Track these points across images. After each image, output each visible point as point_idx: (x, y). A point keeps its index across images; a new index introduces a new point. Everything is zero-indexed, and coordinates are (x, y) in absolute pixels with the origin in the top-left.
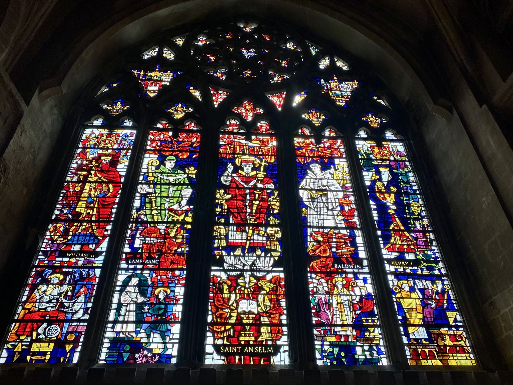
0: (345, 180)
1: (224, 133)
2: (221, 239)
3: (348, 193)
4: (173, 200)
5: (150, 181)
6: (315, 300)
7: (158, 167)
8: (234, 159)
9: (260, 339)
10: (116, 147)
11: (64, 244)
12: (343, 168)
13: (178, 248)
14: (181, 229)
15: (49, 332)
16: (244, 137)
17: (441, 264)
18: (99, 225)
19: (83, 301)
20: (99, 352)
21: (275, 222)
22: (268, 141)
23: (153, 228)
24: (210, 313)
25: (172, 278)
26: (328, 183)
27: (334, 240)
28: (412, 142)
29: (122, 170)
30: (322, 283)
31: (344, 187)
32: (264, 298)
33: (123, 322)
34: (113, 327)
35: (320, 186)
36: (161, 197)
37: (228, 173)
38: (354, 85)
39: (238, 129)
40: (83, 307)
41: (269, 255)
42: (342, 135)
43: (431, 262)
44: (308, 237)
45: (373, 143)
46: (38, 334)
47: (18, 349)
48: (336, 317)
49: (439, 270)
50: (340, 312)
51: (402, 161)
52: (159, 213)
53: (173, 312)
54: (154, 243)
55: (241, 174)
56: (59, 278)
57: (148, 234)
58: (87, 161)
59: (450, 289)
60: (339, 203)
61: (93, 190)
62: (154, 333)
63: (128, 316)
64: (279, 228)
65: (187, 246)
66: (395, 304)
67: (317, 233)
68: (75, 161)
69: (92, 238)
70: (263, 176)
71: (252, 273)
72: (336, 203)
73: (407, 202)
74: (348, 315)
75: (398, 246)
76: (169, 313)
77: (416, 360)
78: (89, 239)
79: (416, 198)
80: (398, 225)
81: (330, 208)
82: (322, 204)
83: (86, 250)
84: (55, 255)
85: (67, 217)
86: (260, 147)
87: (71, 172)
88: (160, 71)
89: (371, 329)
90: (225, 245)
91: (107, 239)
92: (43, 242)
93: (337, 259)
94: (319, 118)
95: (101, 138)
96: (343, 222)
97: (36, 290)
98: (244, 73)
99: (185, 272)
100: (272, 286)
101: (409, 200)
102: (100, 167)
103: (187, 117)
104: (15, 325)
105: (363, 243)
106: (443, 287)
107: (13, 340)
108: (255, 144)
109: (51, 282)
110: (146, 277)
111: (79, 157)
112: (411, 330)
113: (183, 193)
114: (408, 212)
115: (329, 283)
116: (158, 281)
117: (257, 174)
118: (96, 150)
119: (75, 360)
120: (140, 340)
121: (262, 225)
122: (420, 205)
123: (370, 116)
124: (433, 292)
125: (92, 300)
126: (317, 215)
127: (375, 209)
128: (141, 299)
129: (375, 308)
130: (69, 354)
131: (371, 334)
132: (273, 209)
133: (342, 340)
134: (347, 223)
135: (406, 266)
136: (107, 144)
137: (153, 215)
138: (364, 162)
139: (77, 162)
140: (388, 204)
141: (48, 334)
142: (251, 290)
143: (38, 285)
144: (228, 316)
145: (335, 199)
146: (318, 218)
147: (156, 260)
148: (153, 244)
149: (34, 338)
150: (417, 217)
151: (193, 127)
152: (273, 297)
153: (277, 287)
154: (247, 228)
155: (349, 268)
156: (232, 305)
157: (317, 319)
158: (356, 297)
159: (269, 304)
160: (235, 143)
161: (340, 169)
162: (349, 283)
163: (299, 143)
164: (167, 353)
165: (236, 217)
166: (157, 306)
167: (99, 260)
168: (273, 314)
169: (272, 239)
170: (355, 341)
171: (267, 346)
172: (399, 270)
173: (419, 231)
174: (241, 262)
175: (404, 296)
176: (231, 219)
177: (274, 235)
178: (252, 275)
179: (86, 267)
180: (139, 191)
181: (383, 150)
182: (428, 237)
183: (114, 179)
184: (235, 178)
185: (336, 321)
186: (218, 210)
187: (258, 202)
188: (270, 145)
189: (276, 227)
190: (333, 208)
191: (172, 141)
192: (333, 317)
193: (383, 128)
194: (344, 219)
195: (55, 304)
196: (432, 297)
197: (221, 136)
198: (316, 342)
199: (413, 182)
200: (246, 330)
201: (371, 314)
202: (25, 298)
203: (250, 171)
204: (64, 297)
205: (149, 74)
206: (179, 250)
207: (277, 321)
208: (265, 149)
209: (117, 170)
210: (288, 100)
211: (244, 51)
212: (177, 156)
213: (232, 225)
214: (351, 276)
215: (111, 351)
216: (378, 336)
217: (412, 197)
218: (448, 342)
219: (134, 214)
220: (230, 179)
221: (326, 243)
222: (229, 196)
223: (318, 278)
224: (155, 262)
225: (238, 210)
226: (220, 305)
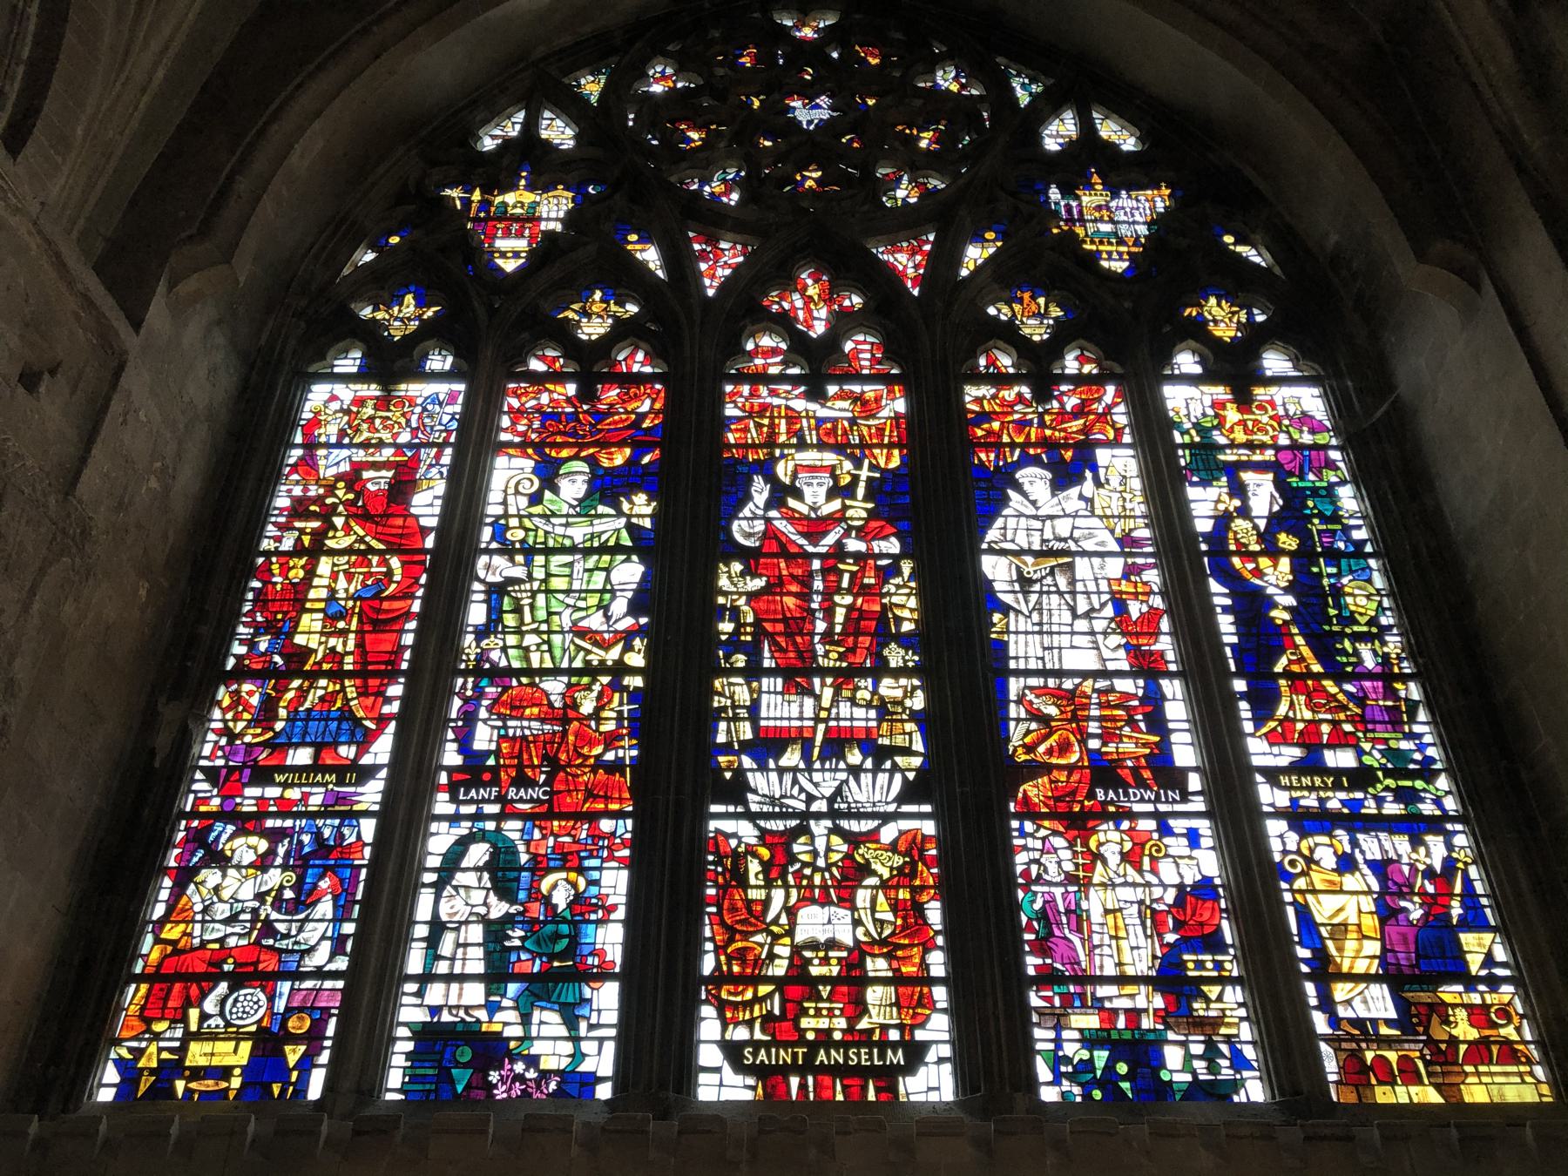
0: (1130, 517)
1: (740, 378)
2: (736, 718)
3: (1140, 561)
4: (585, 599)
5: (513, 543)
6: (1033, 902)
7: (536, 499)
8: (772, 461)
9: (863, 1024)
10: (405, 437)
11: (264, 744)
12: (1124, 477)
13: (605, 751)
14: (614, 691)
15: (234, 1010)
16: (802, 389)
17: (1443, 783)
18: (365, 686)
19: (330, 916)
20: (383, 1067)
21: (905, 661)
22: (878, 399)
23: (529, 690)
24: (709, 946)
25: (589, 841)
26: (1074, 528)
27: (1095, 712)
28: (1349, 383)
29: (429, 511)
30: (1056, 850)
31: (1127, 541)
32: (874, 900)
33: (449, 978)
34: (420, 994)
35: (1048, 541)
36: (548, 592)
37: (753, 508)
38: (1158, 199)
39: (782, 363)
40: (329, 933)
41: (888, 765)
42: (1118, 370)
43: (1412, 775)
44: (1012, 706)
45: (1220, 392)
46: (204, 1017)
47: (149, 1061)
48: (1101, 955)
49: (1438, 802)
50: (1111, 937)
51: (1316, 447)
52: (544, 642)
53: (597, 947)
54: (532, 735)
55: (794, 510)
56: (255, 848)
57: (513, 708)
58: (320, 486)
59: (1474, 862)
60: (1112, 592)
61: (341, 576)
62: (543, 1009)
63: (464, 959)
64: (920, 679)
65: (634, 742)
66: (1290, 911)
67: (1041, 691)
68: (283, 488)
69: (345, 726)
70: (864, 514)
71: (834, 823)
72: (1099, 593)
73: (1332, 581)
74: (1138, 948)
75: (1300, 726)
76: (586, 950)
77: (1356, 1086)
78: (339, 728)
79: (1363, 569)
80: (1302, 659)
81: (1080, 611)
82: (1055, 598)
83: (329, 762)
84: (239, 780)
85: (271, 662)
86: (853, 421)
87: (274, 524)
88: (531, 187)
89: (1213, 991)
90: (749, 735)
91: (392, 726)
92: (204, 741)
93: (1104, 771)
94: (1045, 315)
95: (358, 412)
96: (1122, 653)
97: (192, 886)
98: (799, 178)
99: (629, 822)
100: (898, 861)
101: (1339, 575)
102: (360, 504)
103: (622, 331)
104: (137, 990)
105: (1188, 721)
106: (1449, 857)
107: (134, 1033)
108: (839, 409)
109: (234, 862)
110: (513, 841)
111: (295, 477)
112: (1340, 991)
113: (616, 577)
114: (1335, 616)
115: (1079, 849)
116: (549, 851)
117: (845, 508)
118: (345, 453)
119: (315, 1091)
120: (502, 1032)
121: (863, 672)
122: (1378, 590)
123: (1213, 301)
124: (1417, 870)
125: (355, 914)
126: (1041, 633)
127: (1226, 610)
128: (499, 909)
129: (1225, 924)
130: (295, 1075)
131: (1212, 1005)
132: (899, 620)
133: (1121, 1023)
134: (1136, 657)
135: (1326, 788)
136: (377, 431)
137: (527, 650)
138: (1191, 455)
139: (289, 491)
140: (1270, 590)
141: (234, 1016)
142: (832, 876)
143: (196, 870)
144: (763, 956)
145: (1096, 579)
146: (1042, 643)
147: (541, 787)
148: (531, 739)
149: (193, 1027)
150: (1365, 629)
151: (639, 363)
152: (904, 894)
153: (913, 864)
154: (817, 681)
155: (1142, 800)
156: (775, 921)
157: (1039, 961)
158: (1165, 890)
159: (889, 917)
160: (772, 412)
161: (1115, 482)
162: (1143, 845)
163: (978, 400)
164: (582, 1068)
165: (781, 650)
166: (550, 928)
167: (371, 794)
168: (903, 947)
169: (897, 713)
170: (1161, 1027)
171: (884, 1045)
172: (1303, 802)
173: (1370, 676)
174: (802, 790)
175: (1319, 886)
176: (767, 654)
177: (901, 703)
178: (836, 830)
179: (334, 815)
180: (481, 574)
181: (1253, 413)
182: (1403, 694)
183: (403, 542)
184: (776, 523)
185: (1101, 967)
186: (726, 627)
187: (848, 600)
188: (884, 413)
190: (1093, 610)
191: (576, 413)
192: (1090, 955)
193: (1254, 340)
194: (1128, 643)
195: (248, 925)
196: (1411, 886)
197: (729, 388)
198: (1038, 1033)
199: (1351, 517)
200: (819, 999)
201: (1214, 943)
202: (159, 911)
203: (821, 499)
204: (272, 905)
205: (499, 199)
206: (610, 756)
207: (915, 969)
208: (869, 427)
209: (413, 511)
210: (945, 259)
211: (797, 104)
212: (592, 461)
213: (770, 672)
214: (1148, 825)
215: (417, 1064)
216: (1235, 1013)
217: (1350, 566)
218: (1465, 1031)
219: (469, 647)
220: (760, 526)
221: (1070, 721)
222: (759, 583)
223: (1043, 833)
225: (787, 625)
226: (738, 922)
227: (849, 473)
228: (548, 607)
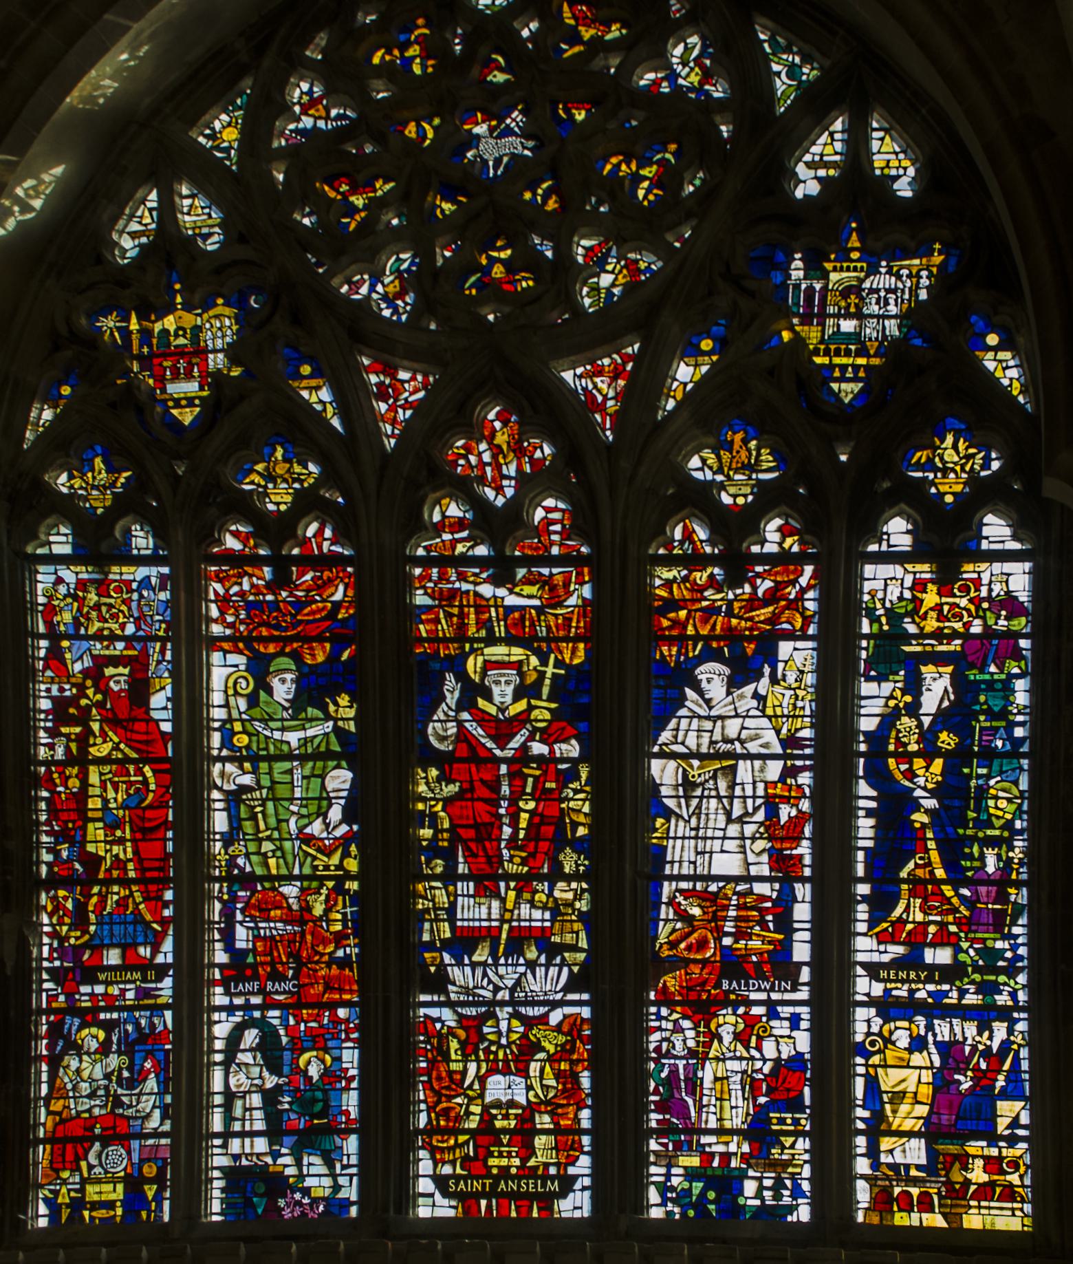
4: (306, 806)
5: (240, 748)
113: (331, 785)
156: (470, 1087)
186: (426, 833)
189: (579, 881)
224: (289, 986)
227: (535, 669)
228: (277, 814)
